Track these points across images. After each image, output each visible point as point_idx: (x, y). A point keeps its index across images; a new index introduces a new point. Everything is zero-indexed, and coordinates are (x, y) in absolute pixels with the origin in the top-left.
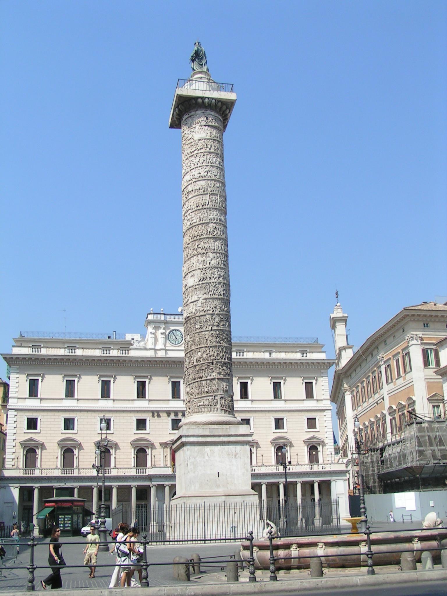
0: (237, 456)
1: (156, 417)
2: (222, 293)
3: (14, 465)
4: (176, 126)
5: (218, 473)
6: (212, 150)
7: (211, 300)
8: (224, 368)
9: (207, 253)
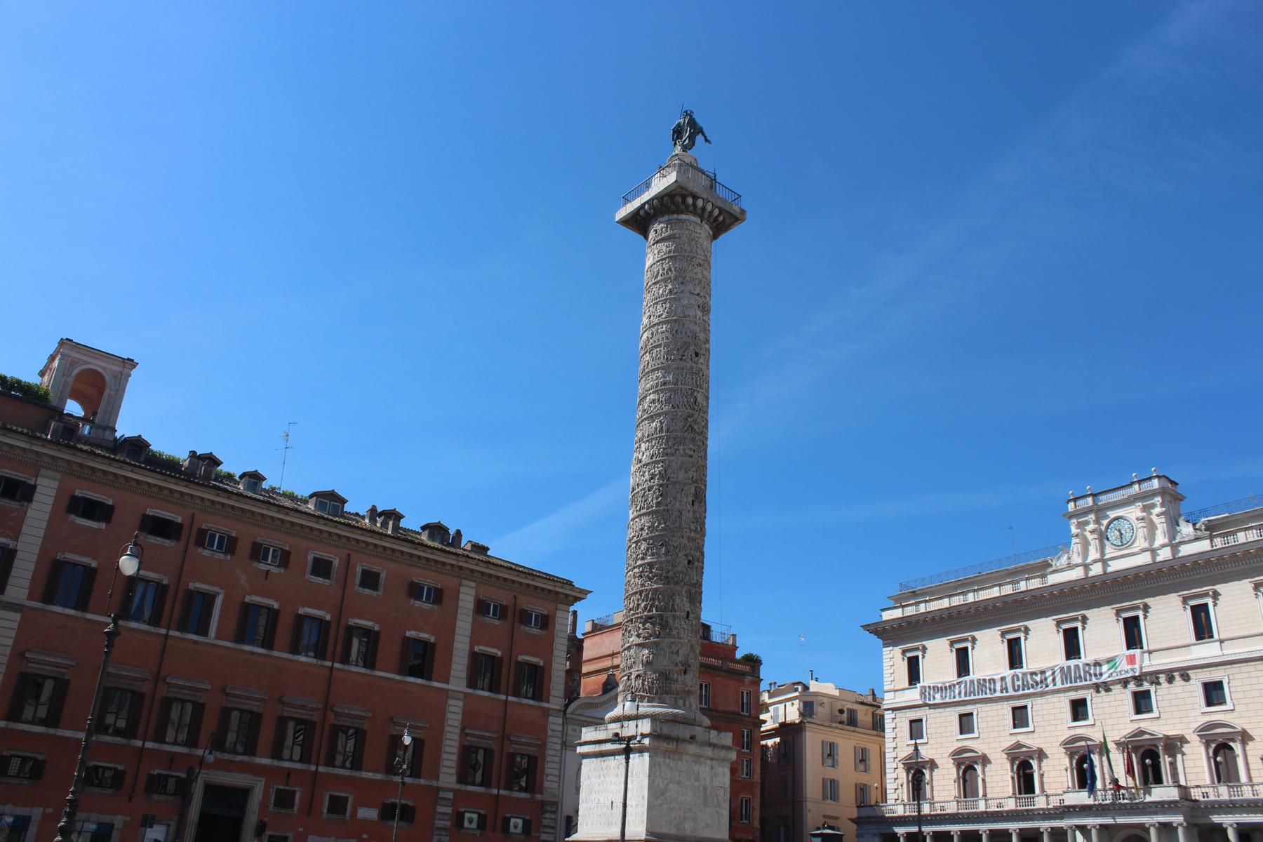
0: (634, 773)
1: (1103, 693)
2: (654, 501)
3: (898, 799)
5: (612, 802)
6: (659, 278)
7: (637, 520)
8: (648, 625)
9: (640, 445)
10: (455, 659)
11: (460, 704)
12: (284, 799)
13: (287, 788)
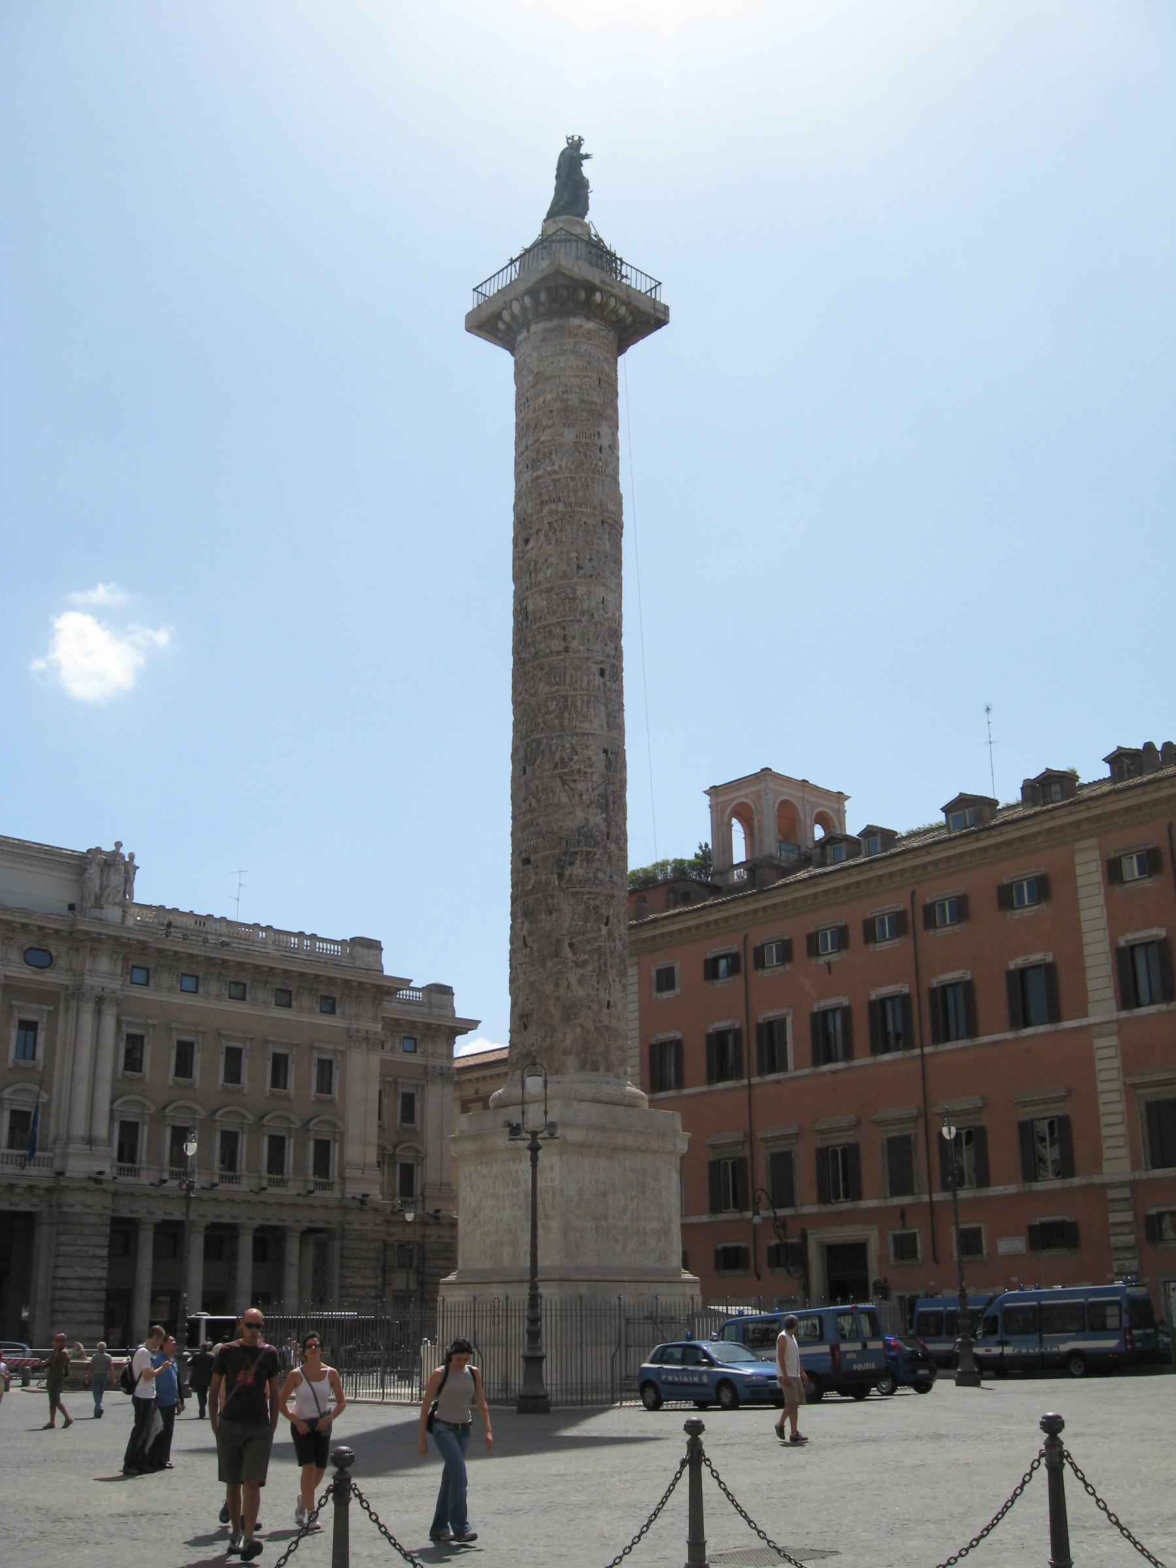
4: (648, 323)
10: (1090, 973)
11: (1113, 1040)
12: (905, 1247)
13: (905, 1232)
